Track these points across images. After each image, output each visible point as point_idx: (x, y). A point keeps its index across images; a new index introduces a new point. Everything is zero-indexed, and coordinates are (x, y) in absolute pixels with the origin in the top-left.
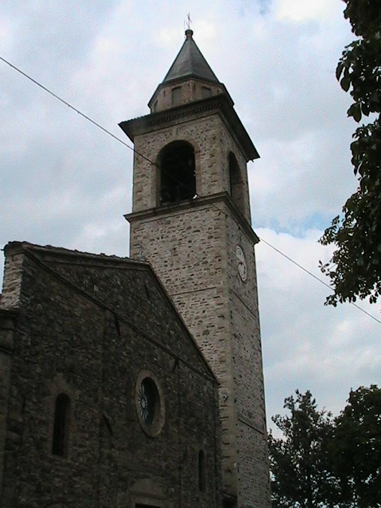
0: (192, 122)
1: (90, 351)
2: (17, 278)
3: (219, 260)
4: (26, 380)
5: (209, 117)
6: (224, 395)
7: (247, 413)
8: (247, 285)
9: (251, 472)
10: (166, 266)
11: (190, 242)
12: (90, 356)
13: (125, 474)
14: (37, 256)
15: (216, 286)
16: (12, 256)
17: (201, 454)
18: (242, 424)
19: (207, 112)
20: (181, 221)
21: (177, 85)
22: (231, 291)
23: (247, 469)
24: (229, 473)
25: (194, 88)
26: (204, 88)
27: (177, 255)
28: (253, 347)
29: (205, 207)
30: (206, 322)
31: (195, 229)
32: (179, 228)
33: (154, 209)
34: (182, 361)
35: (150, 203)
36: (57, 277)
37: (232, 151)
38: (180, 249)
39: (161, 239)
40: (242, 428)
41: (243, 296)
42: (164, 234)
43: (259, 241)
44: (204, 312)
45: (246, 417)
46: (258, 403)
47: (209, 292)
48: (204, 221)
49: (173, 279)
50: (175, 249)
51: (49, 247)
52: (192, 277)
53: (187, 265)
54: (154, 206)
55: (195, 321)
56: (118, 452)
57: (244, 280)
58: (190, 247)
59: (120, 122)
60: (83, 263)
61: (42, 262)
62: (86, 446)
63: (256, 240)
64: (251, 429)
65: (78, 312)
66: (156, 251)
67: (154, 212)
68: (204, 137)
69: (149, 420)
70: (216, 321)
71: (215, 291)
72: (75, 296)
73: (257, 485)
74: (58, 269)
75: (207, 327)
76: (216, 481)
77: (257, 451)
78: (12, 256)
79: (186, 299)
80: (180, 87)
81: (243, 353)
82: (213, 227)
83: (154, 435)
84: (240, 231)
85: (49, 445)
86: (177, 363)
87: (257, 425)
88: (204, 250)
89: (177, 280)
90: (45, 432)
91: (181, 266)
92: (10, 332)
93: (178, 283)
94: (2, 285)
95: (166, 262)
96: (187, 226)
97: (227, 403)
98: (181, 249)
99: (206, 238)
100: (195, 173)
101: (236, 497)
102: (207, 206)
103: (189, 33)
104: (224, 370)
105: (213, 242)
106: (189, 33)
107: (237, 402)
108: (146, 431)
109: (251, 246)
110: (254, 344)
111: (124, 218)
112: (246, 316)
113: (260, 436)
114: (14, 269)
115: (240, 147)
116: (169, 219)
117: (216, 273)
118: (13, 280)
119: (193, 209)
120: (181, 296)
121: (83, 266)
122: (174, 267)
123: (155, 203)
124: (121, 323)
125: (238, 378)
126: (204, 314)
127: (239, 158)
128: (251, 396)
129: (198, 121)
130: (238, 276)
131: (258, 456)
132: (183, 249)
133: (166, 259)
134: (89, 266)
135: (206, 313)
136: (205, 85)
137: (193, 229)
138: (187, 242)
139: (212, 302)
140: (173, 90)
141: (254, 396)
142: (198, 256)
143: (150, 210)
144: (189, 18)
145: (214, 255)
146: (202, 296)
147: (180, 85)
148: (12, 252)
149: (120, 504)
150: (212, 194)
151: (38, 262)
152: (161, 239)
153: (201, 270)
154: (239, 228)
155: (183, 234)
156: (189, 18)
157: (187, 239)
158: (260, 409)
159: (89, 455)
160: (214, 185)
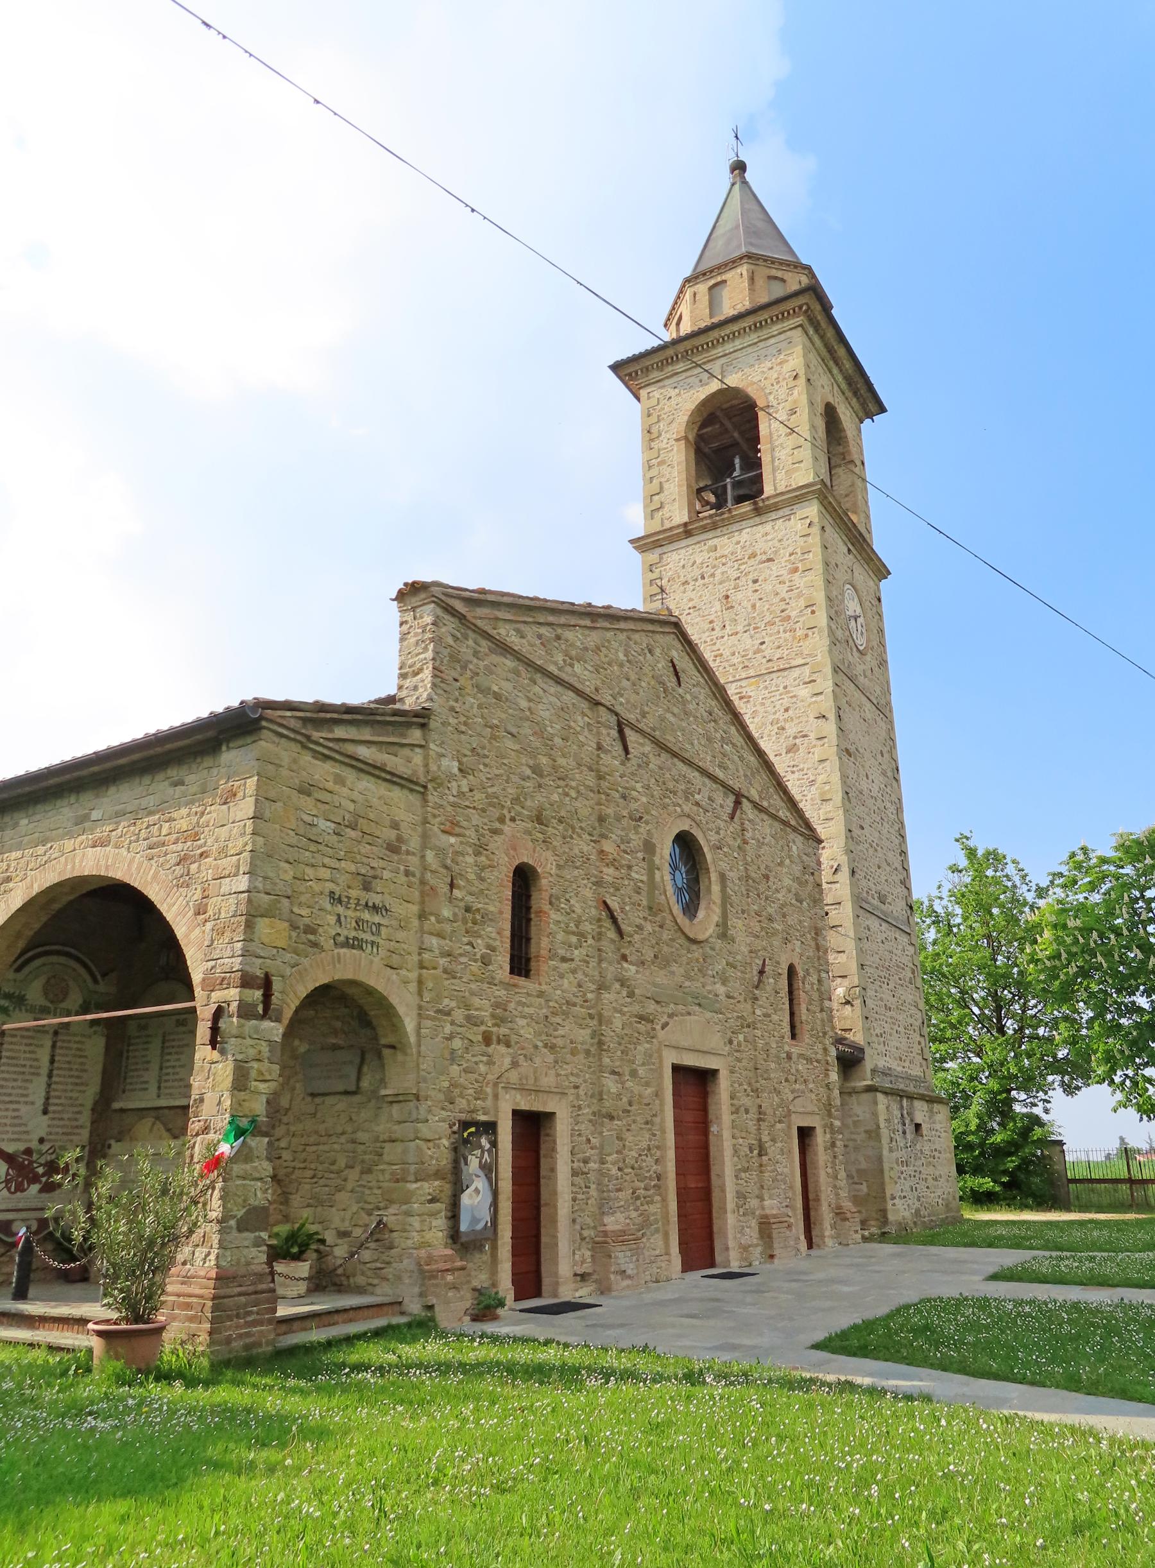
0: (750, 350)
1: (573, 784)
2: (426, 649)
3: (813, 612)
4: (452, 840)
5: (782, 337)
6: (832, 863)
7: (876, 896)
8: (868, 658)
9: (889, 1005)
10: (713, 630)
11: (755, 581)
12: (573, 794)
13: (651, 1007)
14: (459, 606)
15: (808, 660)
16: (414, 609)
17: (791, 970)
18: (868, 915)
19: (779, 326)
20: (738, 543)
21: (719, 279)
22: (836, 670)
23: (881, 999)
24: (848, 1007)
25: (752, 279)
26: (770, 278)
27: (732, 607)
28: (884, 773)
29: (781, 513)
30: (791, 730)
31: (764, 557)
32: (733, 558)
33: (685, 524)
34: (747, 798)
35: (678, 514)
36: (504, 648)
37: (831, 400)
38: (736, 597)
39: (700, 582)
41: (861, 679)
42: (705, 569)
43: (889, 573)
44: (787, 710)
45: (876, 902)
46: (897, 878)
47: (796, 673)
48: (780, 541)
49: (727, 653)
50: (727, 597)
51: (482, 591)
52: (764, 646)
53: (751, 627)
54: (686, 519)
55: (770, 727)
56: (633, 968)
57: (861, 648)
58: (756, 591)
59: (611, 363)
60: (551, 619)
61: (474, 621)
62: (572, 960)
63: (882, 572)
66: (690, 605)
67: (687, 531)
68: (775, 376)
69: (691, 909)
70: (813, 727)
71: (807, 670)
72: (539, 681)
73: (901, 1029)
74: (503, 631)
75: (795, 738)
76: (823, 1020)
77: (898, 966)
78: (414, 609)
79: (753, 688)
80: (724, 282)
81: (864, 785)
82: (798, 551)
83: (701, 937)
84: (851, 556)
85: (503, 960)
86: (737, 803)
87: (897, 919)
88: (783, 594)
89: (733, 654)
90: (493, 935)
91: (740, 628)
92: (418, 750)
93: (735, 660)
94: (397, 666)
95: (711, 622)
96: (750, 552)
97: (837, 877)
98: (740, 596)
99: (784, 572)
100: (759, 451)
101: (862, 1050)
102: (786, 511)
103: (739, 167)
104: (830, 816)
105: (799, 580)
106: (739, 167)
107: (857, 876)
108: (686, 930)
109: (872, 583)
110: (884, 767)
111: (630, 546)
112: (868, 716)
113: (904, 939)
114: (416, 634)
115: (849, 394)
116: (716, 541)
117: (807, 635)
118: (417, 655)
119: (757, 520)
120: (744, 683)
122: (728, 629)
123: (686, 512)
124: (628, 732)
125: (857, 832)
126: (786, 715)
127: (845, 415)
128: (884, 865)
129: (761, 345)
130: (851, 642)
132: (743, 597)
133: (711, 618)
134: (563, 626)
135: (790, 712)
136: (774, 273)
137: (758, 558)
138: (750, 582)
139: (804, 692)
140: (711, 288)
141: (889, 865)
142: (773, 608)
143: (678, 526)
144: (736, 137)
145: (802, 603)
146: (779, 680)
147: (724, 277)
148: (414, 601)
149: (643, 1064)
150: (794, 486)
151: (461, 618)
152: (700, 582)
153: (779, 632)
154: (849, 550)
155: (742, 567)
156: (736, 137)
157: (751, 577)
158: (901, 890)
159: (580, 976)
160: (797, 470)
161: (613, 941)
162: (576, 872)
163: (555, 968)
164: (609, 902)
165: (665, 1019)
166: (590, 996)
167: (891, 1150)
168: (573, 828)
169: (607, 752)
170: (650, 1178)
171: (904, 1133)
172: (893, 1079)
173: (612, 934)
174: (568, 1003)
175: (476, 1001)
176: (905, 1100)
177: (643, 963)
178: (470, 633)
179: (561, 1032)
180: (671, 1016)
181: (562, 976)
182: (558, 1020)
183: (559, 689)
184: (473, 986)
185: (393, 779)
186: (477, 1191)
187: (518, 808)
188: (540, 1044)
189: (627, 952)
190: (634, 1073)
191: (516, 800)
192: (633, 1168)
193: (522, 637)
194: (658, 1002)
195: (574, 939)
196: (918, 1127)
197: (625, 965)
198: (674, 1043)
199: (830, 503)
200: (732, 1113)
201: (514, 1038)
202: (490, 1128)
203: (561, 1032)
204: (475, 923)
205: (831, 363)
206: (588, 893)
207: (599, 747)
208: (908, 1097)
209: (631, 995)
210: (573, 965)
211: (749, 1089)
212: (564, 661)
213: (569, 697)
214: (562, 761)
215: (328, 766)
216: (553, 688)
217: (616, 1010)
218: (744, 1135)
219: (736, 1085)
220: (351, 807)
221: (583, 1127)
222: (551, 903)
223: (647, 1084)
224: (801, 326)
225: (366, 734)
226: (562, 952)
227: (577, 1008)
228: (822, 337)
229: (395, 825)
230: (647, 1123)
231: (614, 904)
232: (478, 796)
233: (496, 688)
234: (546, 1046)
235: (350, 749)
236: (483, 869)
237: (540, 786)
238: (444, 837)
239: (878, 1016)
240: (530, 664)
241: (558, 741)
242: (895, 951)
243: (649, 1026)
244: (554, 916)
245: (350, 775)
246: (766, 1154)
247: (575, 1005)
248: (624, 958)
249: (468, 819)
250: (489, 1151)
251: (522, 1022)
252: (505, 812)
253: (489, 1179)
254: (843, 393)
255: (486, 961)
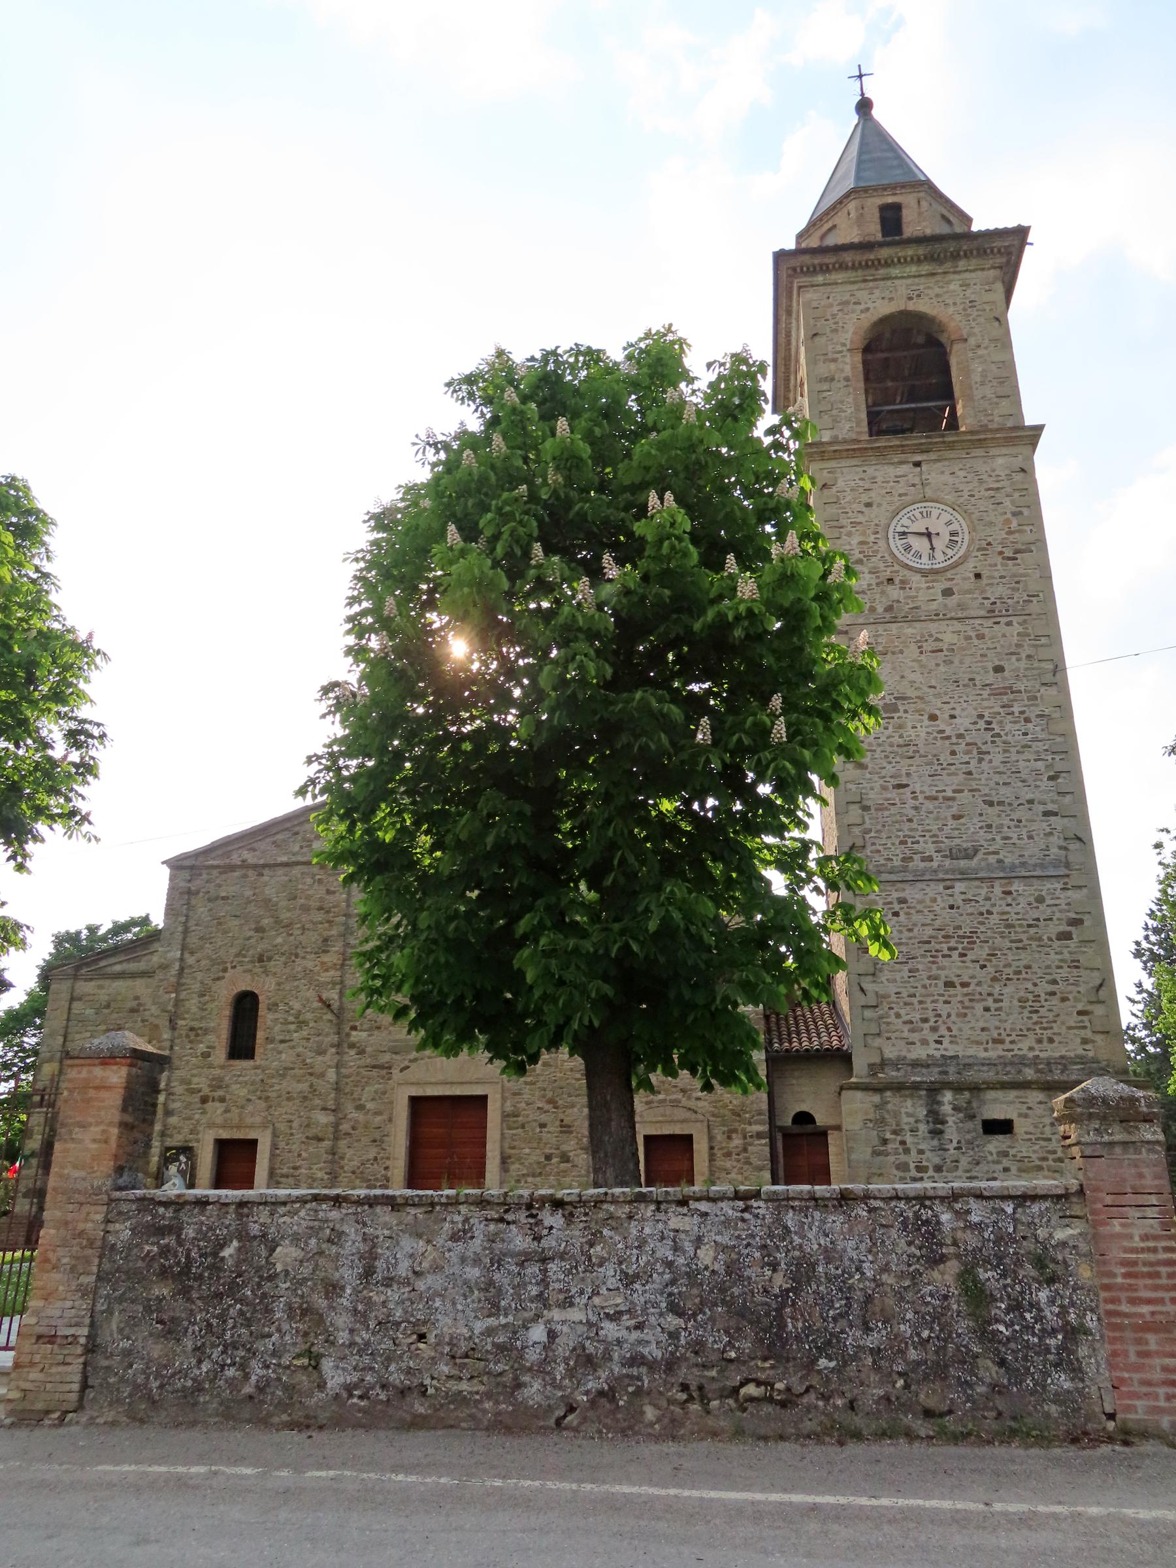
13: (386, 1058)
18: (899, 885)
36: (232, 868)
40: (895, 895)
56: (364, 1034)
64: (959, 887)
65: (269, 892)
115: (948, 266)
121: (287, 829)
131: (1024, 937)
149: (373, 1099)
154: (917, 464)
161: (331, 1021)
162: (296, 984)
163: (273, 1049)
164: (324, 997)
165: (407, 1063)
166: (308, 1061)
167: (876, 1153)
168: (297, 956)
169: (334, 892)
170: (377, 1180)
171: (936, 1133)
172: (952, 1070)
173: (329, 1016)
174: (286, 1068)
175: (195, 1080)
176: (948, 1096)
177: (378, 1028)
178: (204, 872)
179: (277, 1087)
180: (415, 1060)
181: (280, 1053)
182: (274, 1081)
183: (287, 869)
184: (194, 1072)
185: (133, 975)
186: (174, 1184)
187: (241, 959)
188: (253, 1098)
189: (357, 1024)
190: (360, 1108)
191: (237, 955)
192: (354, 1172)
193: (254, 850)
194: (396, 1053)
195: (293, 1027)
196: (1002, 1127)
197: (354, 1033)
198: (414, 1080)
199: (835, 451)
200: (510, 1128)
201: (228, 1097)
202: (187, 1150)
203: (277, 1087)
204: (197, 1035)
205: (882, 272)
206: (311, 994)
207: (328, 892)
208: (958, 1088)
209: (361, 1052)
210: (292, 1044)
211: (547, 1107)
212: (301, 847)
213: (296, 871)
214: (285, 916)
215: (93, 983)
216: (281, 871)
217: (329, 1067)
218: (535, 1145)
219: (523, 1105)
220: (107, 998)
221: (294, 1147)
222: (269, 1009)
223: (376, 1114)
224: (800, 287)
225: (112, 960)
226: (279, 1038)
227: (296, 1071)
228: (843, 267)
229: (137, 998)
230: (375, 1141)
231: (332, 995)
232: (203, 963)
233: (223, 894)
234: (260, 1098)
235: (109, 970)
236: (205, 1004)
237: (262, 938)
238: (167, 996)
239: (915, 1000)
240: (255, 867)
241: (284, 903)
242: (995, 910)
243: (384, 1072)
244: (270, 1016)
245: (107, 983)
246: (568, 1161)
247: (293, 1069)
248: (354, 1028)
249: (195, 978)
250: (186, 1163)
251: (234, 1087)
252: (229, 965)
253: (184, 1176)
254: (933, 274)
255: (206, 1055)
